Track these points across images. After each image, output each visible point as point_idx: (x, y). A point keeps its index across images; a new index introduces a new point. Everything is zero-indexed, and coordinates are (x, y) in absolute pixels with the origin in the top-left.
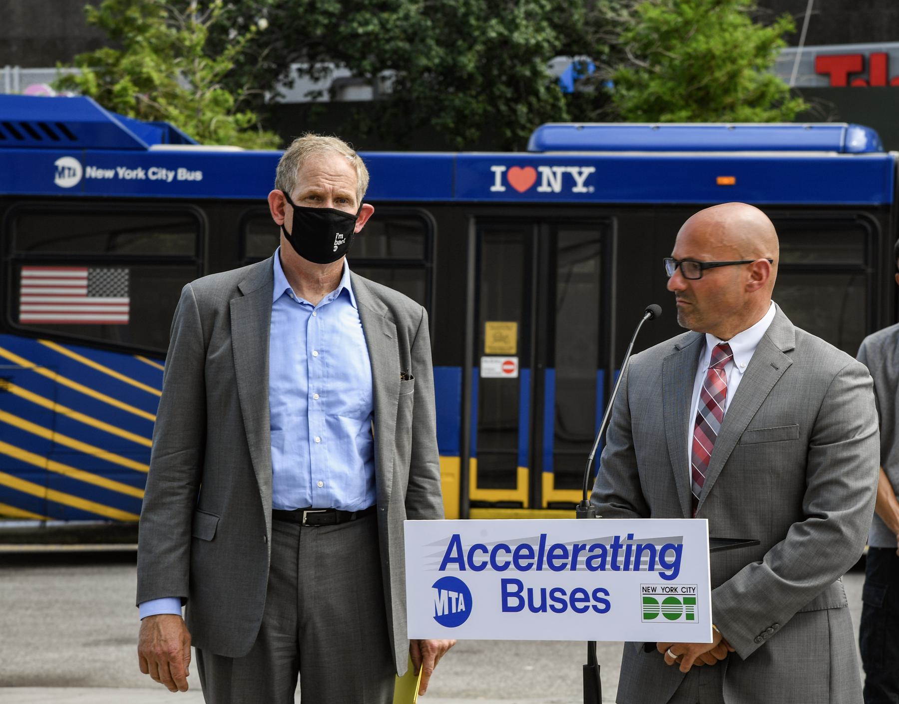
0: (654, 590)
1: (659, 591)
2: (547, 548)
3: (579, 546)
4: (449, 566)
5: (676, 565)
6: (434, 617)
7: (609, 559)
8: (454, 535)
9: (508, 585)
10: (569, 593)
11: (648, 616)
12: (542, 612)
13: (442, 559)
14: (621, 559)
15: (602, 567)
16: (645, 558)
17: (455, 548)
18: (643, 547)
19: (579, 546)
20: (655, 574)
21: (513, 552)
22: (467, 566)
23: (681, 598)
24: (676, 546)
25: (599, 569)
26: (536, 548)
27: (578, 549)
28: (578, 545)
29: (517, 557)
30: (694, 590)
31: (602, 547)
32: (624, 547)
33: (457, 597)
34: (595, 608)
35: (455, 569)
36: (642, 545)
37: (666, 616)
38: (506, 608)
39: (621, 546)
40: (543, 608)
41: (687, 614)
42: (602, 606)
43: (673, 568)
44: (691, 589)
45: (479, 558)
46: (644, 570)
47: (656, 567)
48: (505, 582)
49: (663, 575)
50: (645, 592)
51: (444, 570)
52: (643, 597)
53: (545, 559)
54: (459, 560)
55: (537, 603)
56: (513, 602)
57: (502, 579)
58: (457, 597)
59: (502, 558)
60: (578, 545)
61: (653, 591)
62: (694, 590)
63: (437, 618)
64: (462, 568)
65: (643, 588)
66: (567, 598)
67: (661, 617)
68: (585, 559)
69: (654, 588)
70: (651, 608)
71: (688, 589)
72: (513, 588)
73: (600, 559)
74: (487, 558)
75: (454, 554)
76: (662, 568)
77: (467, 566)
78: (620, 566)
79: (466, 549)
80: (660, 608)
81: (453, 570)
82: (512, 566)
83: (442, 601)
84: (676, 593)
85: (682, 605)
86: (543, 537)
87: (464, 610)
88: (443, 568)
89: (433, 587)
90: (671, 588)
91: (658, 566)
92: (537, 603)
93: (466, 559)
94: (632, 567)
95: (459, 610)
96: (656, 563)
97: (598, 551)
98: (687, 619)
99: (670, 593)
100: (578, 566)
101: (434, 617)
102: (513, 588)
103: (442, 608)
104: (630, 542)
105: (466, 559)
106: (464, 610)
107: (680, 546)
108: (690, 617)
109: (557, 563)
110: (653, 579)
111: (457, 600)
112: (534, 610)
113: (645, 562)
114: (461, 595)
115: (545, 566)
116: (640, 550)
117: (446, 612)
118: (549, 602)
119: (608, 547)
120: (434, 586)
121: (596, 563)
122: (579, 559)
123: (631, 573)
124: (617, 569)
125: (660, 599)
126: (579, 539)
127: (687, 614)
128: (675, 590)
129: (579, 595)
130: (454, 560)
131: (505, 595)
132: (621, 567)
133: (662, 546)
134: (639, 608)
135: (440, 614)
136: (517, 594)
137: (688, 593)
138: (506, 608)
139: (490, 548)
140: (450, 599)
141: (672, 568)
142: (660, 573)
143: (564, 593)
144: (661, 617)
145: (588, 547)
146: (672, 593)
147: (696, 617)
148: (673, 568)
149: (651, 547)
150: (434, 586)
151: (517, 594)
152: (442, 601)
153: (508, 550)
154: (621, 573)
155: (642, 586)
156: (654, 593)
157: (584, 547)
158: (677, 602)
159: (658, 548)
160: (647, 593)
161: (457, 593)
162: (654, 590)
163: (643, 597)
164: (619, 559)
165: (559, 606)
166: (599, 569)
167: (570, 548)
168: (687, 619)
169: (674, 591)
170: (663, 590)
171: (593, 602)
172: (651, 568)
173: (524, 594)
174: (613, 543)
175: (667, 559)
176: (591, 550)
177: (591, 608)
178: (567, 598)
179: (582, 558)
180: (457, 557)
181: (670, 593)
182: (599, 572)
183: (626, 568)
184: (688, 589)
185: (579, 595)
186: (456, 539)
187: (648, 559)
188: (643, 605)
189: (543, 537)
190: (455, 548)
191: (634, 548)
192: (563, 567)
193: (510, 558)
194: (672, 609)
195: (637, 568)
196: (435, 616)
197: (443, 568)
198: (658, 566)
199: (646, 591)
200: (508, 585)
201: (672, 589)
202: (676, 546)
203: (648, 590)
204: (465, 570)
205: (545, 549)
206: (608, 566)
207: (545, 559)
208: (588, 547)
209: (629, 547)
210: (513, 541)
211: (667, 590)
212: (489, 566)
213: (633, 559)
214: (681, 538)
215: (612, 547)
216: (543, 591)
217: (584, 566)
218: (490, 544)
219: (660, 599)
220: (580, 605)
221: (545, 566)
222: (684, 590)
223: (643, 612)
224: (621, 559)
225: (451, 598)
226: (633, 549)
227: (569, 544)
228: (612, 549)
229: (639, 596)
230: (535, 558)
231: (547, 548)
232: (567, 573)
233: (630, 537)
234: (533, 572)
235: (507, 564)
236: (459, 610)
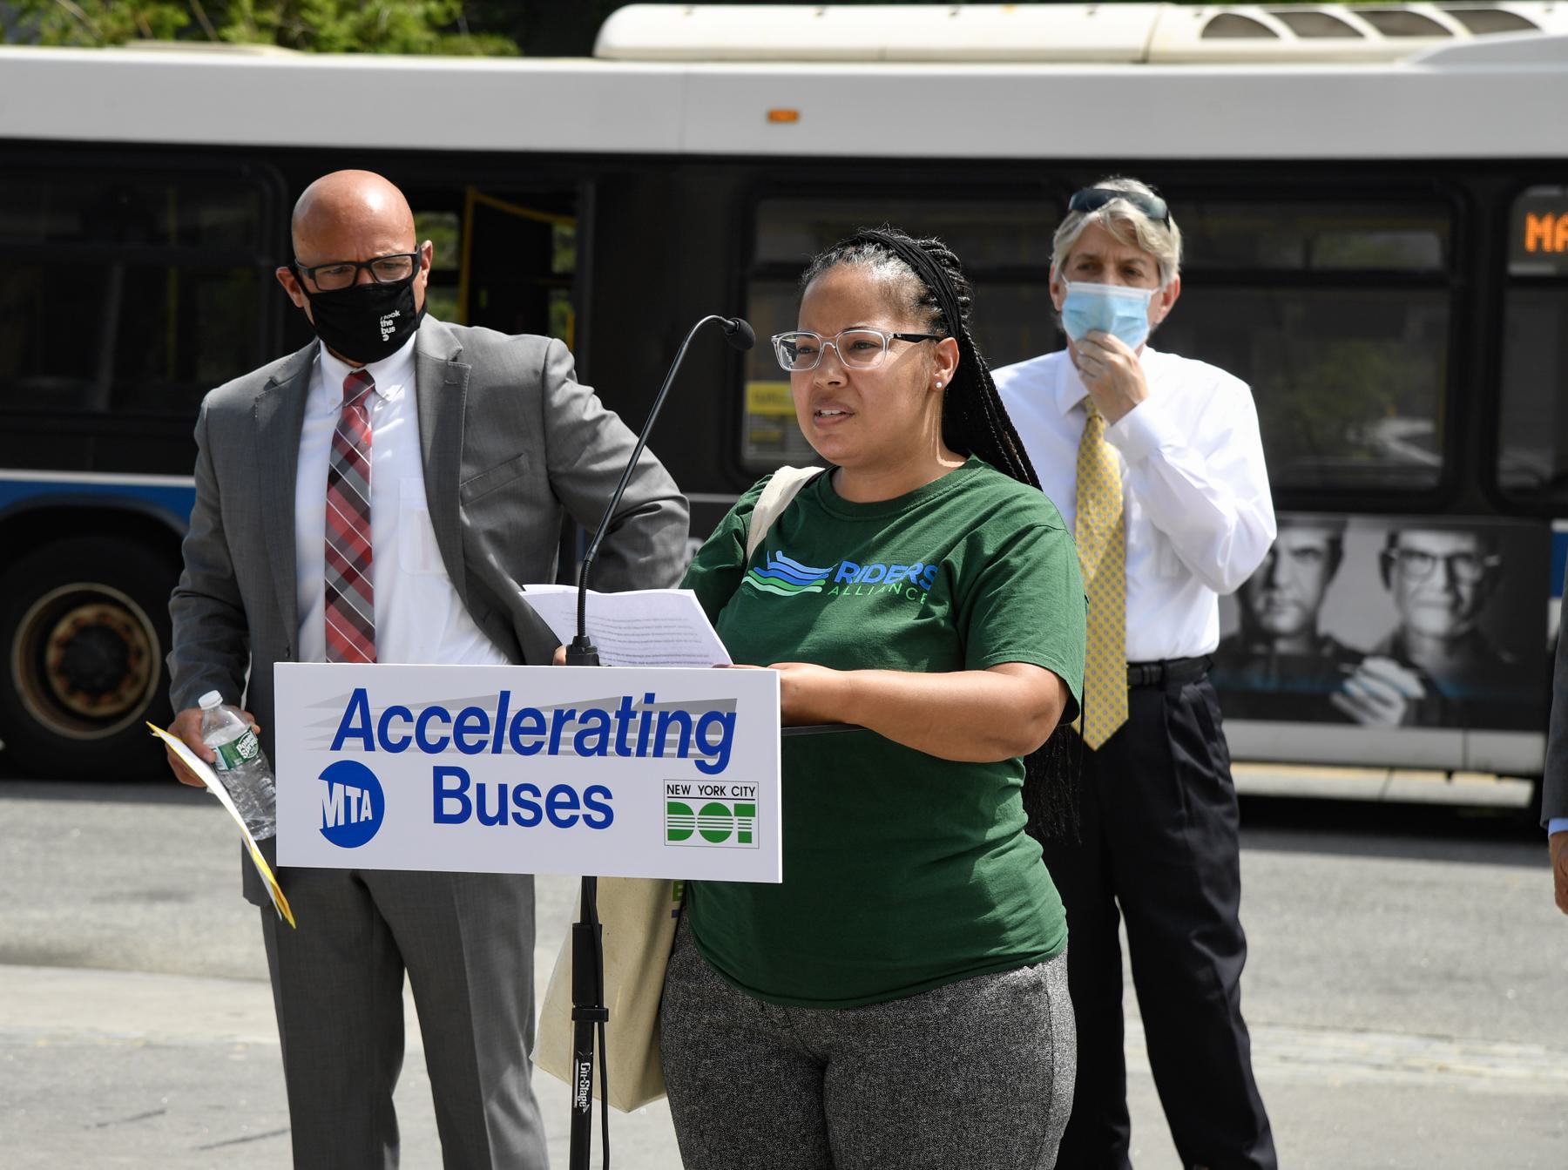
0: (686, 790)
1: (695, 792)
5: (725, 749)
6: (321, 830)
7: (613, 736)
10: (545, 793)
13: (335, 731)
14: (633, 736)
15: (601, 750)
16: (673, 736)
17: (357, 712)
22: (377, 743)
23: (730, 805)
24: (725, 715)
26: (492, 715)
27: (561, 717)
28: (562, 711)
29: (460, 729)
30: (752, 792)
31: (603, 715)
32: (639, 716)
34: (588, 819)
36: (668, 713)
38: (440, 817)
39: (634, 715)
40: (502, 818)
41: (739, 832)
42: (599, 817)
43: (719, 753)
44: (748, 789)
45: (398, 729)
46: (672, 755)
47: (691, 751)
48: (439, 772)
50: (671, 794)
51: (339, 749)
53: (507, 733)
54: (365, 733)
55: (492, 809)
56: (452, 806)
61: (684, 793)
62: (752, 792)
63: (326, 832)
64: (369, 746)
65: (668, 786)
66: (541, 802)
67: (696, 837)
68: (573, 735)
69: (686, 787)
70: (681, 822)
71: (744, 790)
72: (451, 783)
73: (598, 736)
74: (410, 730)
75: (356, 723)
77: (377, 743)
79: (376, 713)
80: (696, 822)
81: (353, 750)
82: (452, 745)
83: (334, 803)
84: (723, 796)
87: (370, 818)
88: (337, 746)
91: (694, 750)
92: (492, 809)
93: (375, 731)
94: (650, 750)
95: (362, 819)
96: (690, 744)
97: (596, 722)
98: (740, 841)
99: (712, 796)
100: (561, 748)
101: (321, 830)
104: (648, 707)
105: (375, 731)
108: (745, 837)
109: (527, 740)
110: (683, 770)
111: (360, 801)
112: (485, 820)
113: (672, 743)
114: (366, 793)
115: (507, 745)
116: (665, 721)
117: (341, 822)
118: (512, 807)
119: (612, 716)
120: (322, 777)
122: (563, 734)
123: (650, 761)
125: (697, 806)
126: (564, 700)
127: (739, 832)
128: (722, 791)
129: (562, 797)
130: (355, 733)
131: (440, 794)
134: (660, 821)
135: (331, 824)
136: (458, 794)
137: (744, 797)
138: (440, 817)
139: (416, 714)
142: (696, 762)
144: (696, 837)
145: (578, 715)
146: (716, 796)
148: (719, 753)
149: (682, 717)
150: (322, 777)
152: (334, 803)
154: (633, 760)
155: (667, 783)
156: (686, 795)
157: (571, 714)
158: (725, 811)
159: (696, 718)
161: (359, 790)
162: (686, 790)
167: (549, 716)
168: (740, 841)
169: (719, 792)
170: (701, 790)
171: (584, 810)
172: (683, 753)
173: (471, 793)
176: (584, 720)
177: (581, 819)
178: (541, 802)
179: (568, 734)
180: (361, 727)
181: (712, 796)
182: (595, 758)
183: (641, 752)
184: (744, 790)
185: (562, 797)
187: (677, 737)
189: (505, 696)
190: (357, 712)
191: (655, 717)
192: (536, 748)
193: (448, 731)
194: (715, 823)
195: (658, 752)
197: (337, 746)
198: (694, 750)
199: (673, 793)
201: (716, 789)
202: (725, 715)
203: (677, 790)
205: (508, 716)
206: (611, 748)
207: (507, 733)
208: (578, 715)
209: (647, 716)
210: (454, 703)
212: (414, 744)
213: (652, 736)
214: (734, 702)
216: (503, 789)
217: (572, 748)
218: (416, 706)
219: (697, 806)
221: (507, 745)
222: (736, 791)
224: (633, 736)
225: (350, 797)
227: (547, 709)
229: (661, 800)
231: (511, 715)
232: (542, 758)
233: (650, 698)
234: (486, 756)
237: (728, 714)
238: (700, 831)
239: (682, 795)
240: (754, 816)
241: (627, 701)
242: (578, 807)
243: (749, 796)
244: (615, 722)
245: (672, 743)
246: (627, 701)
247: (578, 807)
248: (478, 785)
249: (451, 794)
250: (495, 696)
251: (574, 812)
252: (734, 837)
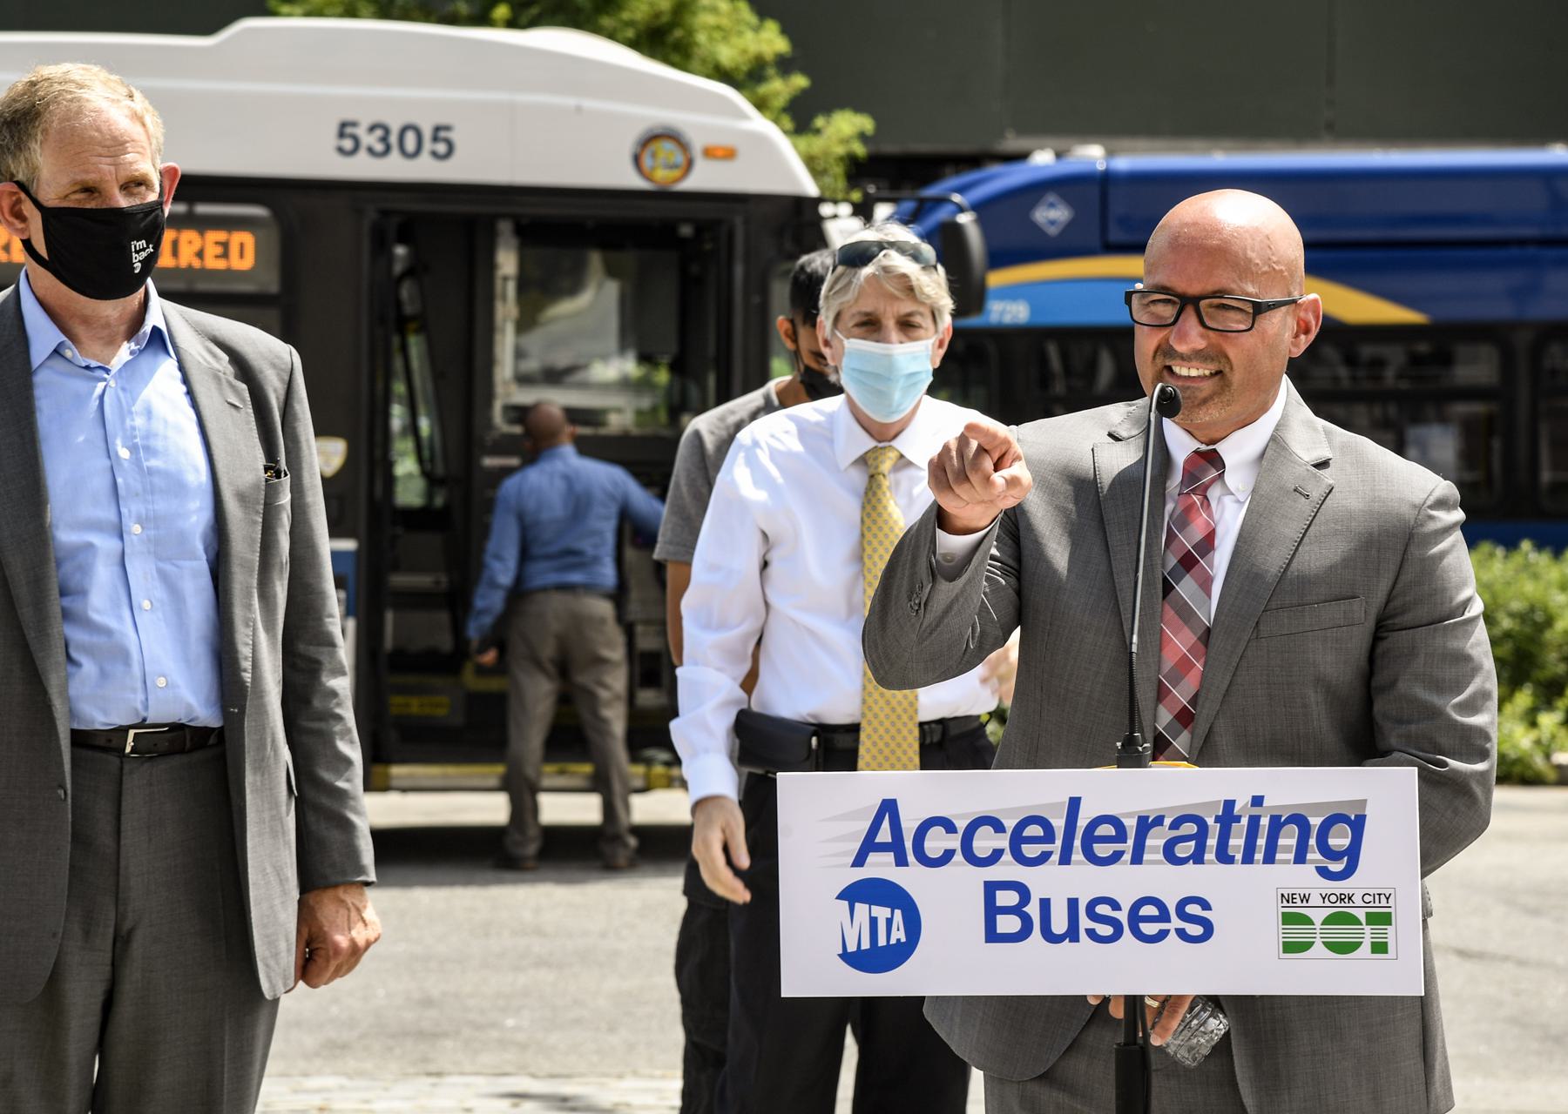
0: (1305, 898)
1: (1315, 900)
2: (1082, 823)
3: (1150, 820)
4: (873, 857)
5: (1352, 854)
6: (839, 955)
7: (1212, 842)
8: (884, 800)
9: (999, 894)
10: (1126, 907)
11: (1290, 948)
12: (1070, 941)
13: (857, 845)
14: (1237, 842)
15: (1198, 858)
16: (1288, 840)
17: (886, 824)
18: (1283, 819)
19: (1150, 820)
20: (1308, 870)
21: (1009, 832)
22: (911, 858)
23: (1361, 914)
24: (1353, 818)
25: (1191, 861)
26: (1059, 824)
27: (1146, 825)
28: (1148, 817)
29: (1017, 839)
30: (1388, 899)
31: (1200, 822)
32: (1245, 821)
33: (889, 916)
34: (1182, 934)
35: (887, 864)
36: (1281, 816)
37: (1331, 946)
38: (992, 936)
39: (1238, 819)
40: (1072, 934)
41: (1372, 942)
42: (1195, 930)
43: (1346, 858)
44: (1382, 896)
45: (936, 843)
46: (1286, 862)
47: (1309, 856)
48: (991, 888)
49: (1324, 872)
50: (1285, 904)
51: (862, 866)
52: (1283, 913)
53: (1077, 843)
54: (896, 847)
55: (1059, 924)
56: (1010, 924)
57: (985, 882)
58: (889, 916)
59: (985, 842)
60: (1148, 817)
61: (1302, 901)
62: (1388, 899)
63: (846, 956)
64: (901, 861)
65: (1283, 895)
66: (1122, 916)
67: (1318, 949)
68: (1161, 842)
69: (1304, 895)
70: (1298, 933)
71: (1377, 897)
72: (1007, 898)
73: (1193, 843)
74: (954, 842)
75: (885, 835)
76: (1322, 858)
77: (911, 858)
78: (1234, 856)
80: (1318, 933)
81: (880, 866)
82: (1007, 857)
83: (857, 925)
84: (1351, 904)
85: (1364, 926)
86: (1075, 804)
87: (903, 940)
88: (859, 861)
89: (837, 898)
90: (1341, 894)
91: (1314, 855)
92: (1059, 924)
93: (908, 845)
94: (1259, 856)
95: (893, 941)
96: (1309, 849)
97: (1190, 828)
98: (1373, 952)
99: (1338, 904)
100: (1146, 857)
101: (839, 955)
102: (1007, 898)
103: (857, 936)
104: (1256, 811)
105: (908, 845)
106: (903, 940)
107: (1361, 819)
108: (1380, 948)
109: (1102, 850)
110: (1305, 878)
111: (889, 922)
112: (1050, 937)
113: (1287, 849)
114: (898, 913)
115: (1078, 855)
116: (1276, 825)
117: (866, 945)
118: (1085, 922)
119: (1210, 821)
120: (840, 897)
122: (1149, 842)
123: (1258, 869)
124: (1230, 860)
125: (1318, 916)
126: (1150, 804)
127: (1372, 942)
128: (1350, 899)
130: (883, 847)
132: (1236, 858)
133: (1323, 819)
134: (1272, 932)
135: (852, 948)
136: (1016, 910)
137: (1377, 904)
138: (992, 936)
139: (961, 825)
140: (873, 922)
141: (1342, 858)
143: (1115, 906)
144: (1318, 949)
145: (1167, 822)
146: (1343, 904)
147: (1391, 947)
148: (1346, 858)
149: (1300, 820)
150: (840, 897)
151: (1016, 910)
152: (857, 925)
153: (998, 827)
154: (1238, 869)
155: (1280, 891)
157: (1159, 821)
159: (1316, 821)
160: (1291, 904)
161: (889, 910)
162: (1305, 898)
163: (1283, 913)
164: (1232, 842)
165: (1105, 930)
166: (1191, 861)
167: (1131, 824)
168: (1373, 952)
169: (1346, 900)
170: (1324, 899)
171: (1176, 923)
172: (1300, 858)
173: (1033, 910)
174: (1220, 814)
175: (1332, 842)
176: (1175, 825)
177: (1173, 934)
178: (1122, 916)
179: (1155, 841)
180: (890, 841)
181: (1338, 904)
182: (1190, 866)
183: (1248, 858)
184: (1377, 897)
186: (889, 808)
187: (1293, 842)
188: (1281, 926)
189: (1075, 804)
190: (886, 824)
191: (1265, 821)
192: (1116, 857)
193: (1003, 842)
194: (1342, 933)
195: (1269, 858)
196: (841, 952)
197: (859, 861)
198: (1314, 855)
199: (1288, 902)
200: (999, 894)
201: (1343, 897)
202: (1353, 818)
203: (1293, 899)
204: (907, 865)
205: (1078, 824)
206: (1210, 856)
207: (1077, 843)
208: (1167, 822)
209: (1254, 821)
210: (1010, 812)
211: (1333, 898)
213: (1261, 842)
214: (1363, 803)
215: (1218, 819)
216: (1073, 904)
217: (1160, 857)
218: (960, 817)
219: (1318, 916)
220: (1149, 929)
221: (1078, 855)
222: (1367, 898)
223: (1281, 940)
224: (1237, 842)
225: (876, 918)
226: (1262, 823)
227: (1129, 815)
228: (1219, 825)
229: (1272, 911)
230: (1056, 842)
231: (1082, 823)
232: (1124, 868)
233: (1257, 801)
234: (1052, 868)
235: (996, 855)
236: (893, 941)
237: (1356, 816)
238: (1323, 942)
239: (1299, 904)
240: (1391, 925)
241: (1229, 805)
242: (1168, 920)
243: (1384, 902)
244: (1214, 829)
245: (1287, 849)
246: (1229, 805)
247: (1168, 920)
248: (1042, 901)
249: (1006, 910)
250: (1063, 803)
251: (1164, 926)
252: (1366, 948)
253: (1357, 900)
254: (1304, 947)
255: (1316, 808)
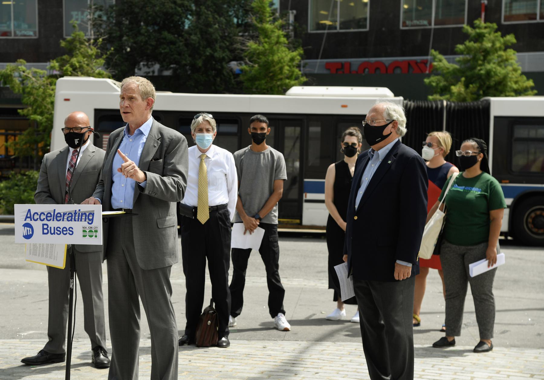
0: (86, 228)
4: (27, 219)
5: (92, 220)
7: (73, 217)
10: (62, 229)
14: (77, 217)
15: (71, 220)
16: (84, 217)
17: (29, 213)
20: (86, 222)
22: (32, 219)
26: (52, 214)
27: (64, 214)
29: (47, 217)
31: (71, 214)
32: (78, 214)
35: (29, 220)
38: (44, 233)
39: (77, 213)
40: (54, 233)
42: (71, 233)
45: (36, 217)
46: (83, 221)
47: (87, 220)
48: (43, 225)
49: (88, 223)
53: (55, 217)
54: (30, 217)
55: (52, 232)
56: (46, 231)
63: (24, 236)
64: (31, 220)
66: (61, 230)
67: (88, 236)
72: (45, 227)
73: (71, 218)
74: (38, 217)
75: (29, 216)
77: (32, 219)
81: (28, 221)
82: (45, 219)
86: (55, 210)
88: (25, 220)
91: (87, 220)
92: (52, 232)
93: (32, 217)
94: (80, 220)
97: (70, 215)
102: (45, 227)
104: (79, 212)
105: (32, 217)
107: (94, 213)
108: (96, 236)
109: (58, 219)
110: (85, 224)
111: (29, 230)
112: (52, 234)
114: (31, 229)
115: (55, 220)
116: (82, 214)
117: (26, 234)
118: (56, 231)
119: (73, 214)
121: (70, 219)
122: (65, 217)
123: (80, 222)
125: (88, 231)
129: (65, 229)
130: (29, 217)
131: (43, 229)
134: (81, 234)
135: (24, 235)
136: (47, 229)
138: (44, 233)
139: (39, 214)
140: (27, 230)
144: (88, 236)
145: (67, 214)
149: (85, 214)
151: (47, 229)
154: (77, 222)
157: (66, 213)
159: (87, 214)
162: (86, 228)
164: (76, 217)
167: (62, 214)
171: (68, 232)
172: (85, 221)
173: (49, 229)
176: (68, 214)
177: (68, 233)
178: (61, 230)
179: (66, 217)
182: (70, 221)
183: (78, 221)
185: (65, 229)
186: (29, 210)
187: (84, 218)
189: (55, 210)
190: (29, 213)
191: (80, 214)
192: (60, 220)
194: (91, 234)
195: (81, 221)
197: (25, 220)
198: (87, 220)
206: (73, 220)
207: (55, 217)
208: (67, 214)
209: (79, 214)
213: (80, 217)
216: (54, 228)
217: (66, 220)
218: (39, 212)
219: (88, 231)
221: (55, 220)
222: (94, 228)
227: (62, 213)
229: (82, 229)
231: (56, 214)
232: (61, 222)
233: (79, 210)
234: (51, 221)
241: (76, 211)
246: (76, 211)
249: (45, 229)
251: (67, 232)
252: (94, 236)
253: (93, 228)
254: (86, 236)
255: (88, 211)
